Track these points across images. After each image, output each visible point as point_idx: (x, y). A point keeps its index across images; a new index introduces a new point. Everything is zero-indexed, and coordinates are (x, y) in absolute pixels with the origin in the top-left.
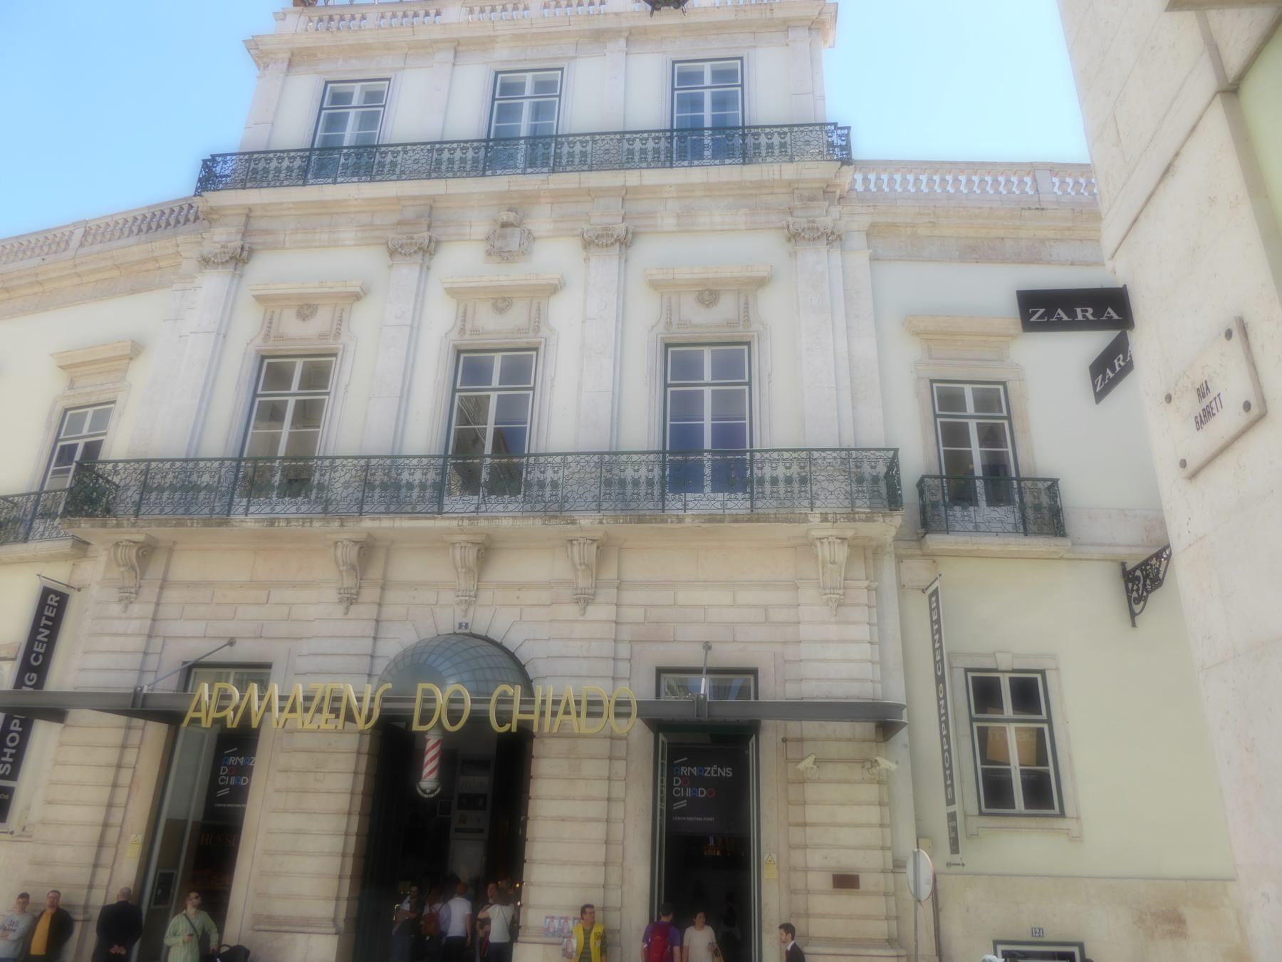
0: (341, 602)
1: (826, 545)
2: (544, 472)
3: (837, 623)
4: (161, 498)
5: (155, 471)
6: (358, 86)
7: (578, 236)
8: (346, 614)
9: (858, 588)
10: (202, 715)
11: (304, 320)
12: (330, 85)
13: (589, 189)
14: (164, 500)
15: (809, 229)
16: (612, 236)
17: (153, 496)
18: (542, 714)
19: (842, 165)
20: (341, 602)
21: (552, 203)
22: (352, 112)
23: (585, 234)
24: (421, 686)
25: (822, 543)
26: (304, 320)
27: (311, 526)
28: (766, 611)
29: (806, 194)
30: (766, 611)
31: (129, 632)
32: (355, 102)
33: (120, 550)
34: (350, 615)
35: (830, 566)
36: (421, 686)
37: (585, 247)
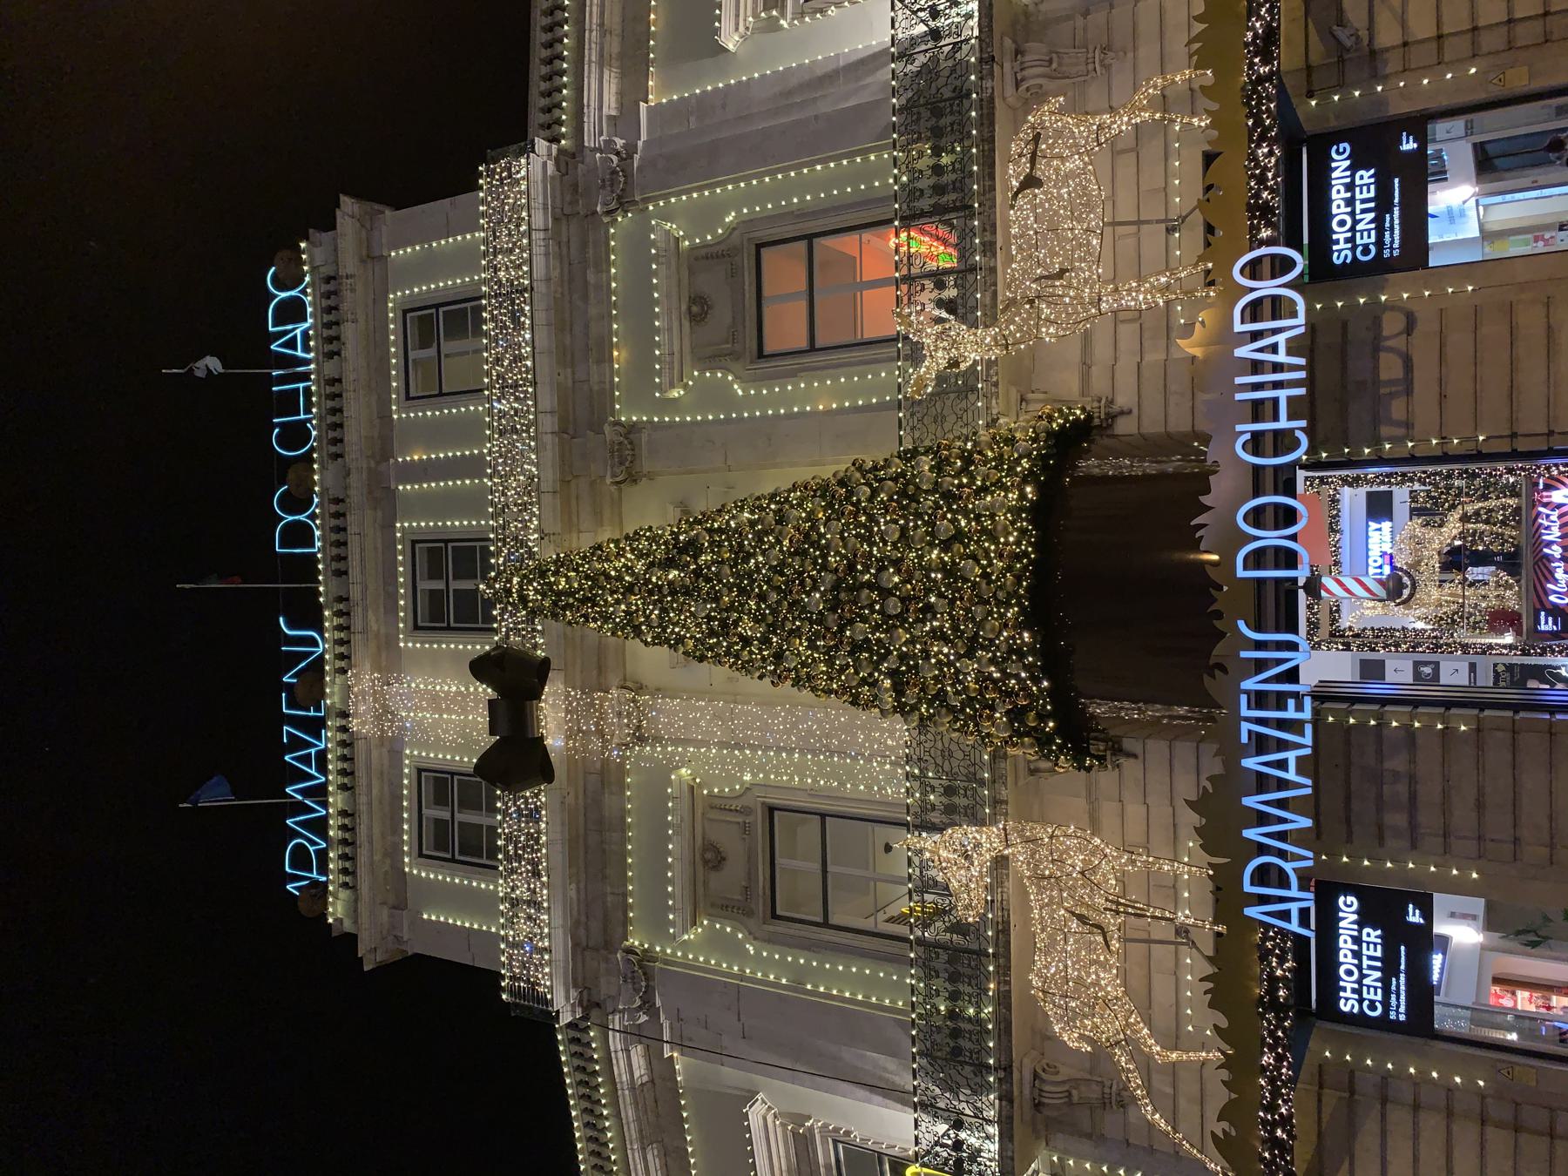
0: (1118, 766)
1: (1026, 73)
2: (921, 172)
3: (1135, 49)
4: (970, 1032)
5: (928, 1044)
6: (424, 811)
7: (620, 490)
8: (1135, 756)
9: (1085, 29)
10: (1294, 908)
11: (724, 859)
12: (425, 852)
13: (562, 481)
14: (972, 1047)
15: (612, 185)
16: (620, 443)
17: (965, 1044)
18: (1277, 385)
19: (534, 152)
20: (1118, 766)
21: (579, 532)
22: (459, 817)
23: (618, 479)
24: (1241, 573)
25: (1023, 80)
26: (724, 859)
27: (1006, 803)
28: (1123, 151)
29: (568, 198)
30: (1123, 151)
31: (1169, 1090)
32: (446, 815)
33: (1046, 1101)
34: (1138, 749)
35: (1054, 65)
36: (1241, 573)
37: (635, 481)
